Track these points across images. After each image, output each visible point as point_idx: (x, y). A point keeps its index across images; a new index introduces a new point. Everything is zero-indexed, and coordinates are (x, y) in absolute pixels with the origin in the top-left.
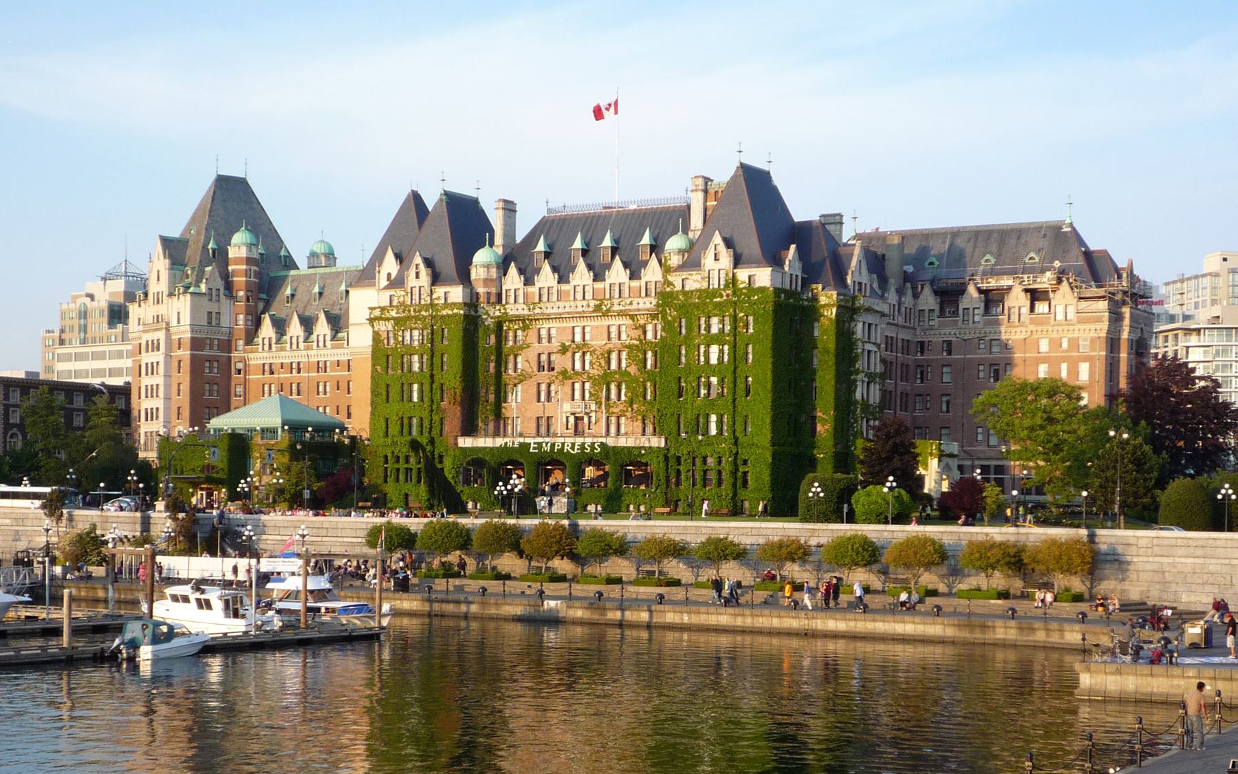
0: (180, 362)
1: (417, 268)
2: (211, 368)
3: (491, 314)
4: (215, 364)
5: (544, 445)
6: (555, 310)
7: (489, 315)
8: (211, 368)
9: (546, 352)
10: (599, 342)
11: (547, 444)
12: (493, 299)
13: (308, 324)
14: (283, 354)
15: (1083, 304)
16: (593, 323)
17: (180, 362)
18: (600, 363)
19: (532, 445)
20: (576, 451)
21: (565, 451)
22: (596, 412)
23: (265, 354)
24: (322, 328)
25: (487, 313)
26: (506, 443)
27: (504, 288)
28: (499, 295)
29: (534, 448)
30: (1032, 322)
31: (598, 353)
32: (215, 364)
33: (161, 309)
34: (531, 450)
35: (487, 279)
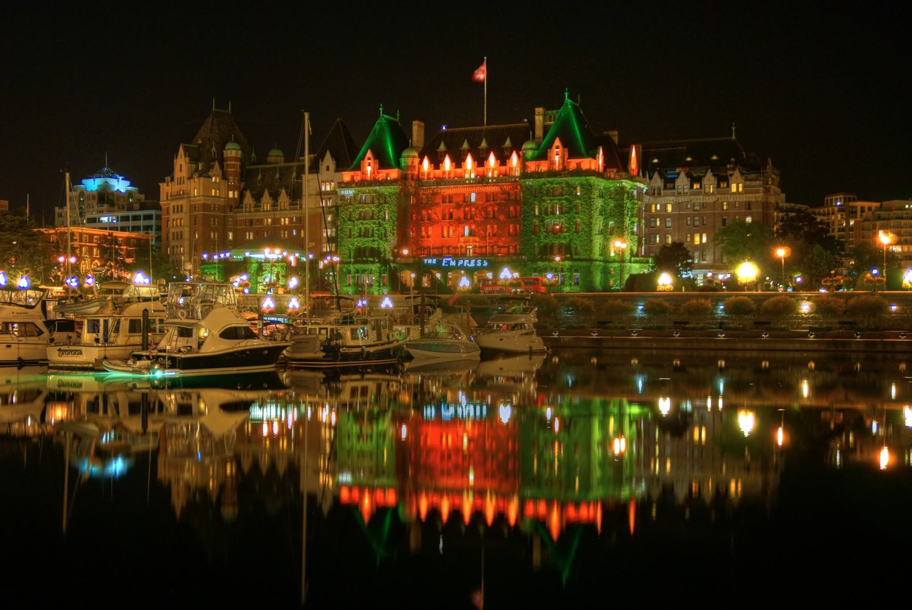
0: (195, 218)
2: (214, 221)
3: (413, 185)
4: (217, 219)
7: (412, 186)
8: (214, 221)
13: (275, 196)
14: (259, 213)
15: (748, 183)
17: (195, 218)
18: (481, 214)
19: (444, 262)
21: (465, 265)
23: (247, 214)
24: (284, 199)
25: (411, 186)
29: (446, 264)
30: (719, 193)
31: (480, 208)
32: (217, 219)
33: (184, 187)
34: (443, 265)
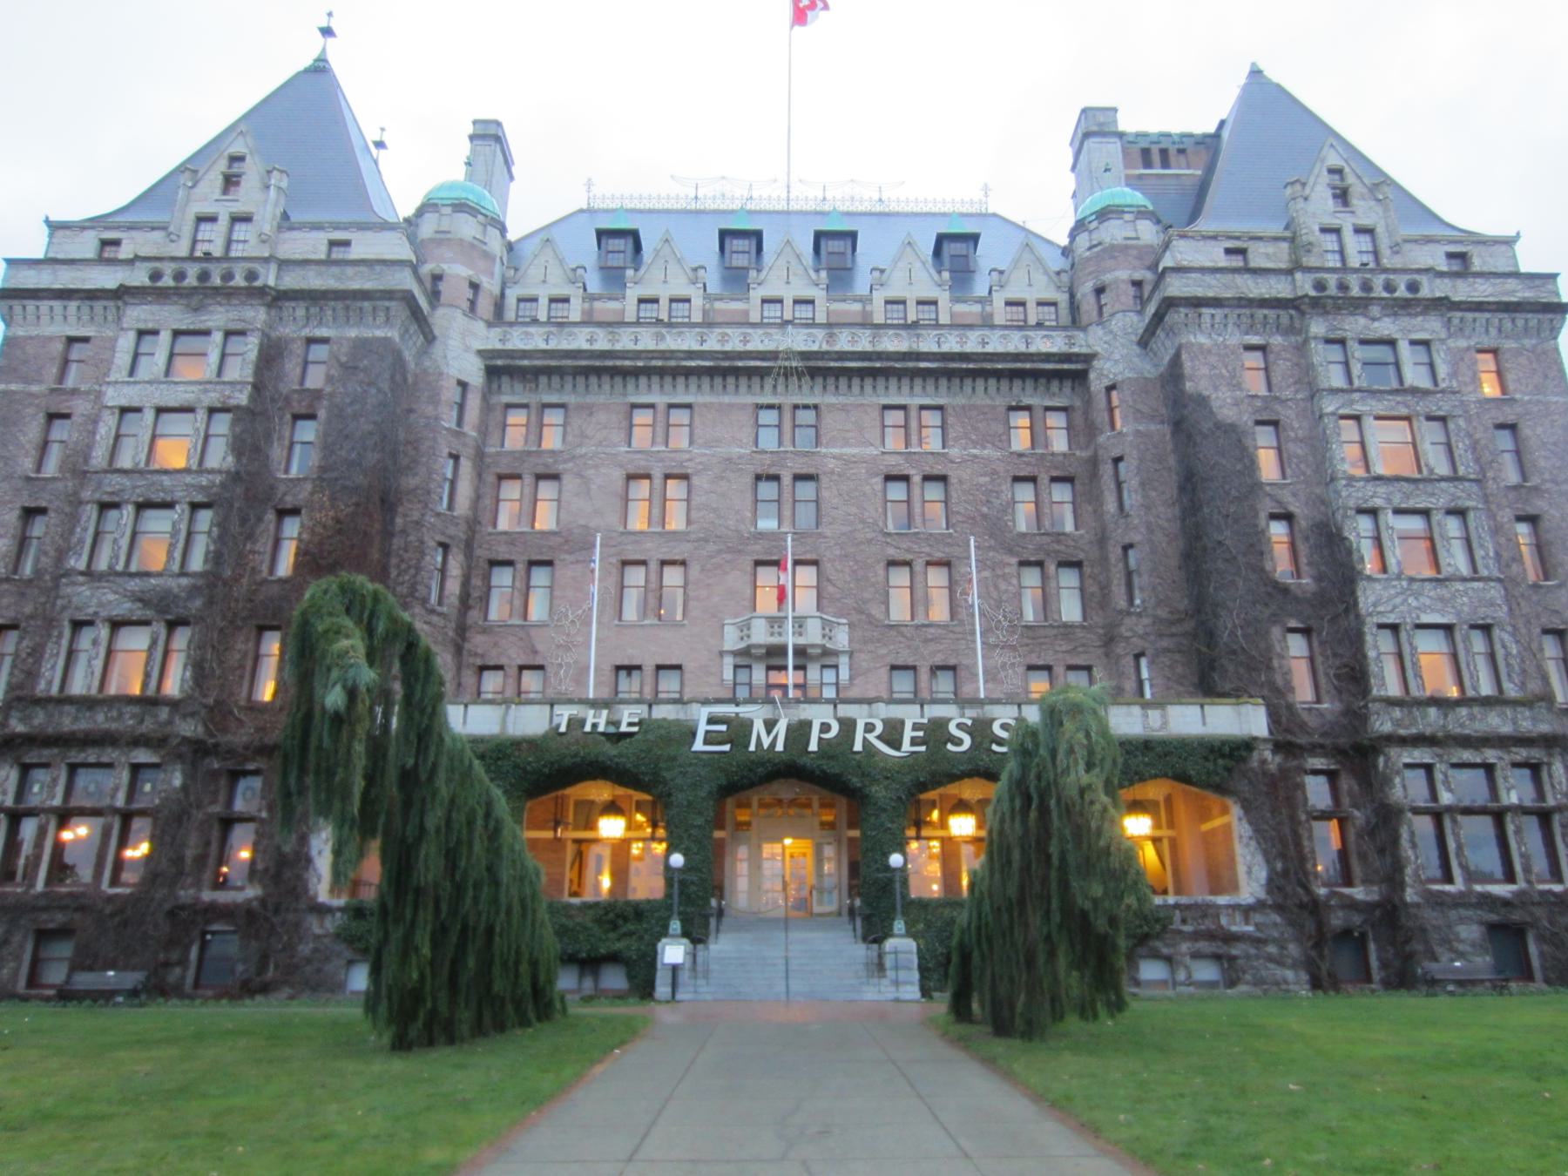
1: (230, 167)
5: (759, 727)
6: (712, 344)
9: (657, 474)
10: (855, 451)
11: (770, 725)
12: (485, 306)
16: (831, 399)
19: (702, 728)
20: (906, 746)
21: (858, 747)
22: (851, 654)
26: (576, 723)
27: (512, 295)
28: (499, 306)
34: (698, 745)
35: (472, 246)
